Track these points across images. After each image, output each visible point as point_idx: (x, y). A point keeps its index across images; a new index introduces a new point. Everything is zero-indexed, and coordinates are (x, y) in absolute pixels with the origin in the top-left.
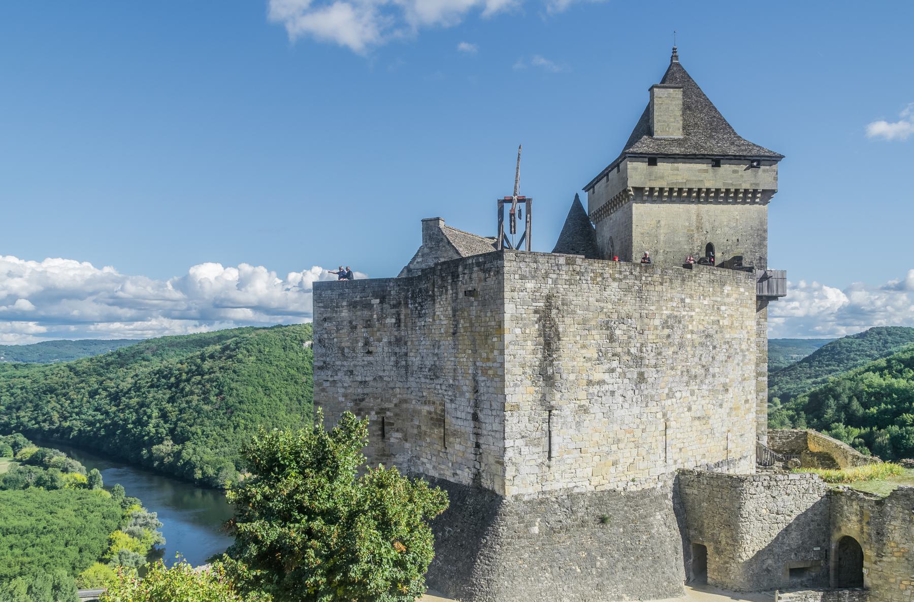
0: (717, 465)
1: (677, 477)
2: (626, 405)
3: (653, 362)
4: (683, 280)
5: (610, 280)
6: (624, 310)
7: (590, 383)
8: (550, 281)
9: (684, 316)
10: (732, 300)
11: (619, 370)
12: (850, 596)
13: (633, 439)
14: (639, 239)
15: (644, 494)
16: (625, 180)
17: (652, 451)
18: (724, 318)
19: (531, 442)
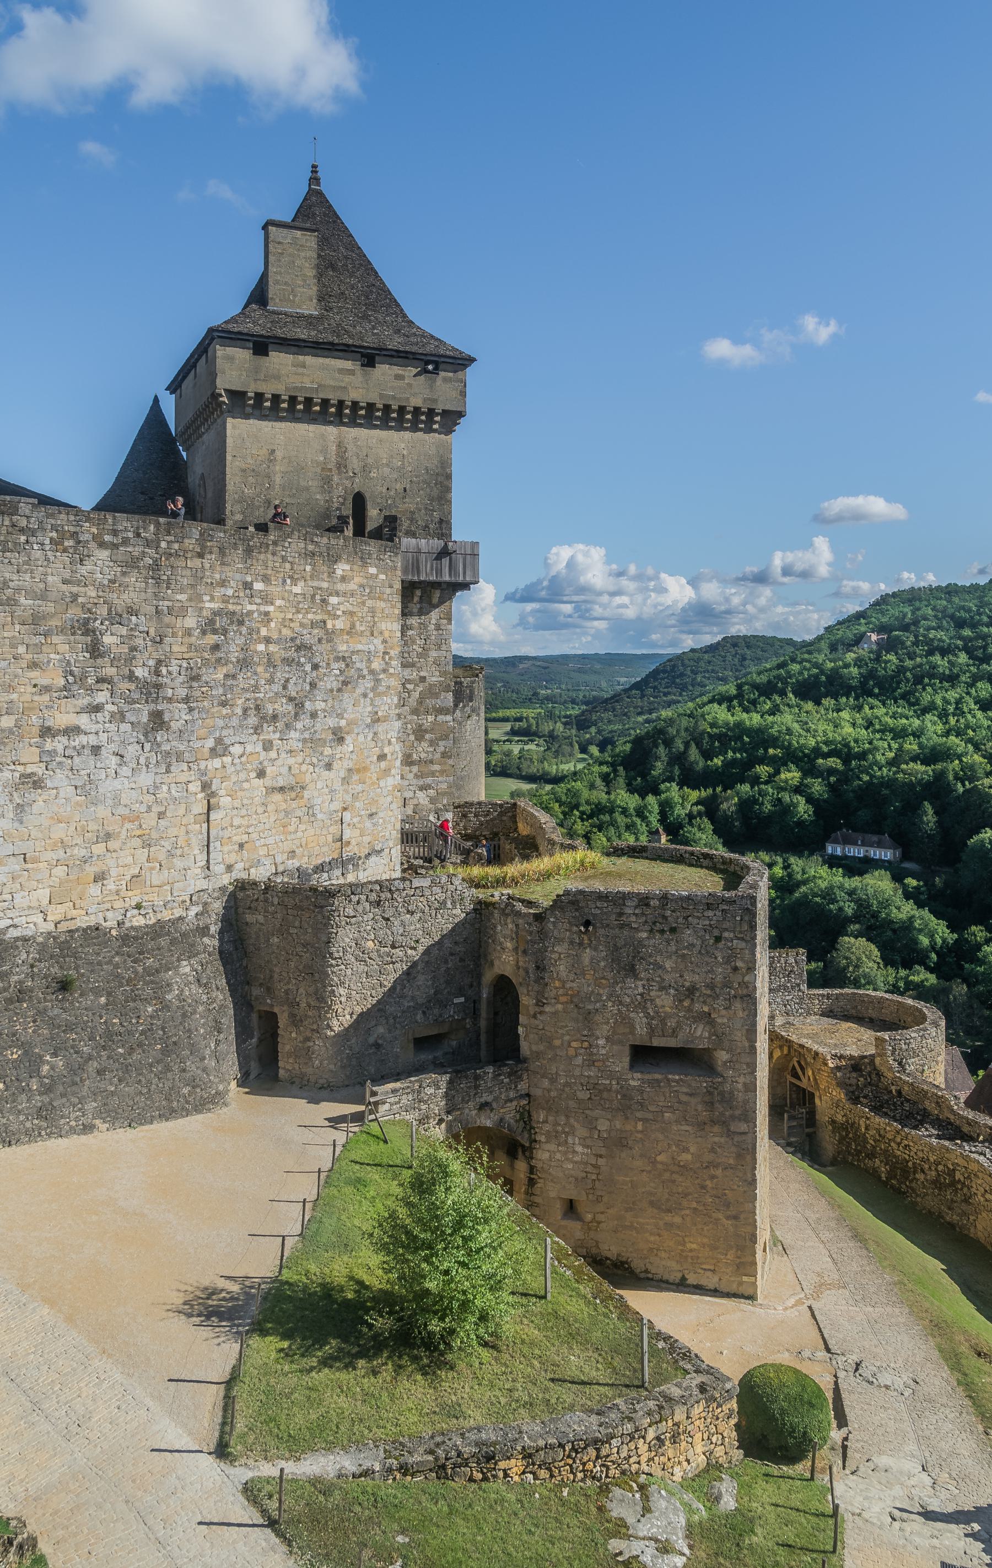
0: (320, 869)
1: (233, 895)
2: (125, 771)
3: (183, 692)
11: (110, 707)
13: (139, 832)
14: (238, 479)
16: (213, 375)
17: (179, 852)
18: (336, 617)
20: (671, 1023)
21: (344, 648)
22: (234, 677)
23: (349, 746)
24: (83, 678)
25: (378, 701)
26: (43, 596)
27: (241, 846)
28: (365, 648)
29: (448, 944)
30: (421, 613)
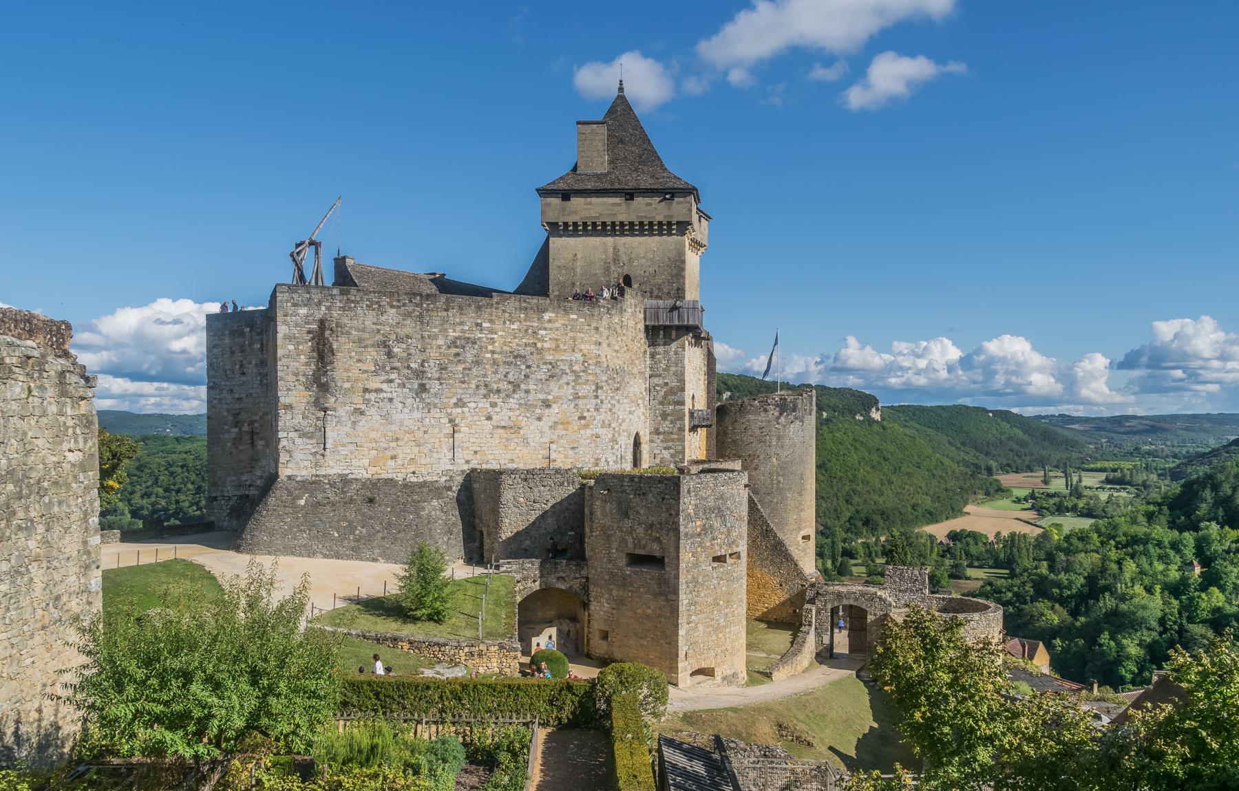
2: (406, 410)
3: (437, 375)
4: (479, 308)
5: (387, 307)
6: (402, 332)
7: (366, 390)
8: (323, 308)
10: (557, 325)
12: (567, 565)
15: (423, 485)
18: (544, 341)
19: (303, 435)
20: (643, 542)
23: (555, 408)
24: (384, 367)
25: (578, 387)
26: (363, 330)
27: (476, 452)
29: (565, 504)
30: (665, 344)
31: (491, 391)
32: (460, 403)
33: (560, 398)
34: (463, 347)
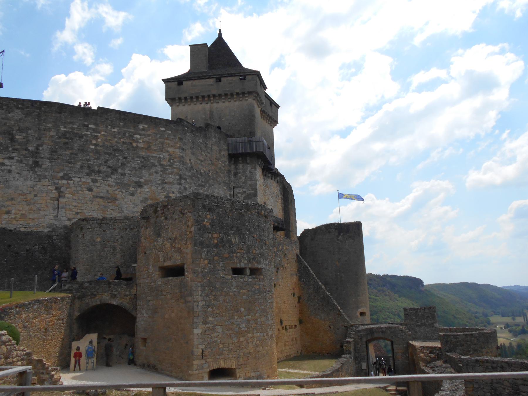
2: (21, 179)
3: (48, 156)
9: (86, 135)
10: (149, 133)
18: (138, 142)
21: (144, 154)
22: (76, 154)
23: (146, 189)
27: (77, 213)
28: (158, 156)
31: (93, 171)
32: (67, 177)
33: (151, 181)
34: (72, 139)
